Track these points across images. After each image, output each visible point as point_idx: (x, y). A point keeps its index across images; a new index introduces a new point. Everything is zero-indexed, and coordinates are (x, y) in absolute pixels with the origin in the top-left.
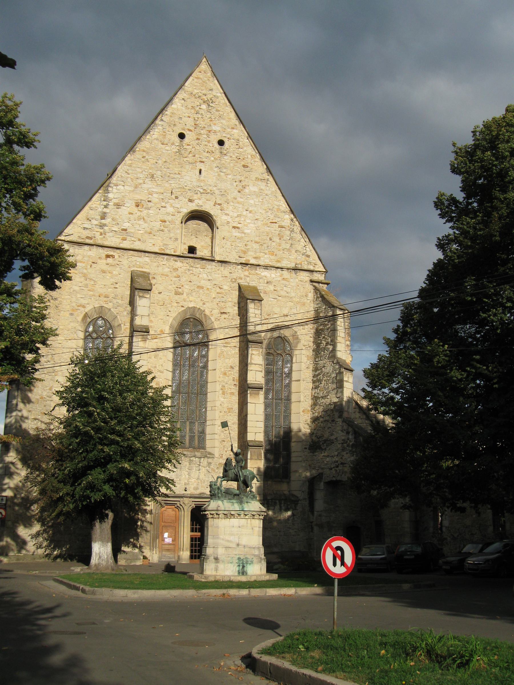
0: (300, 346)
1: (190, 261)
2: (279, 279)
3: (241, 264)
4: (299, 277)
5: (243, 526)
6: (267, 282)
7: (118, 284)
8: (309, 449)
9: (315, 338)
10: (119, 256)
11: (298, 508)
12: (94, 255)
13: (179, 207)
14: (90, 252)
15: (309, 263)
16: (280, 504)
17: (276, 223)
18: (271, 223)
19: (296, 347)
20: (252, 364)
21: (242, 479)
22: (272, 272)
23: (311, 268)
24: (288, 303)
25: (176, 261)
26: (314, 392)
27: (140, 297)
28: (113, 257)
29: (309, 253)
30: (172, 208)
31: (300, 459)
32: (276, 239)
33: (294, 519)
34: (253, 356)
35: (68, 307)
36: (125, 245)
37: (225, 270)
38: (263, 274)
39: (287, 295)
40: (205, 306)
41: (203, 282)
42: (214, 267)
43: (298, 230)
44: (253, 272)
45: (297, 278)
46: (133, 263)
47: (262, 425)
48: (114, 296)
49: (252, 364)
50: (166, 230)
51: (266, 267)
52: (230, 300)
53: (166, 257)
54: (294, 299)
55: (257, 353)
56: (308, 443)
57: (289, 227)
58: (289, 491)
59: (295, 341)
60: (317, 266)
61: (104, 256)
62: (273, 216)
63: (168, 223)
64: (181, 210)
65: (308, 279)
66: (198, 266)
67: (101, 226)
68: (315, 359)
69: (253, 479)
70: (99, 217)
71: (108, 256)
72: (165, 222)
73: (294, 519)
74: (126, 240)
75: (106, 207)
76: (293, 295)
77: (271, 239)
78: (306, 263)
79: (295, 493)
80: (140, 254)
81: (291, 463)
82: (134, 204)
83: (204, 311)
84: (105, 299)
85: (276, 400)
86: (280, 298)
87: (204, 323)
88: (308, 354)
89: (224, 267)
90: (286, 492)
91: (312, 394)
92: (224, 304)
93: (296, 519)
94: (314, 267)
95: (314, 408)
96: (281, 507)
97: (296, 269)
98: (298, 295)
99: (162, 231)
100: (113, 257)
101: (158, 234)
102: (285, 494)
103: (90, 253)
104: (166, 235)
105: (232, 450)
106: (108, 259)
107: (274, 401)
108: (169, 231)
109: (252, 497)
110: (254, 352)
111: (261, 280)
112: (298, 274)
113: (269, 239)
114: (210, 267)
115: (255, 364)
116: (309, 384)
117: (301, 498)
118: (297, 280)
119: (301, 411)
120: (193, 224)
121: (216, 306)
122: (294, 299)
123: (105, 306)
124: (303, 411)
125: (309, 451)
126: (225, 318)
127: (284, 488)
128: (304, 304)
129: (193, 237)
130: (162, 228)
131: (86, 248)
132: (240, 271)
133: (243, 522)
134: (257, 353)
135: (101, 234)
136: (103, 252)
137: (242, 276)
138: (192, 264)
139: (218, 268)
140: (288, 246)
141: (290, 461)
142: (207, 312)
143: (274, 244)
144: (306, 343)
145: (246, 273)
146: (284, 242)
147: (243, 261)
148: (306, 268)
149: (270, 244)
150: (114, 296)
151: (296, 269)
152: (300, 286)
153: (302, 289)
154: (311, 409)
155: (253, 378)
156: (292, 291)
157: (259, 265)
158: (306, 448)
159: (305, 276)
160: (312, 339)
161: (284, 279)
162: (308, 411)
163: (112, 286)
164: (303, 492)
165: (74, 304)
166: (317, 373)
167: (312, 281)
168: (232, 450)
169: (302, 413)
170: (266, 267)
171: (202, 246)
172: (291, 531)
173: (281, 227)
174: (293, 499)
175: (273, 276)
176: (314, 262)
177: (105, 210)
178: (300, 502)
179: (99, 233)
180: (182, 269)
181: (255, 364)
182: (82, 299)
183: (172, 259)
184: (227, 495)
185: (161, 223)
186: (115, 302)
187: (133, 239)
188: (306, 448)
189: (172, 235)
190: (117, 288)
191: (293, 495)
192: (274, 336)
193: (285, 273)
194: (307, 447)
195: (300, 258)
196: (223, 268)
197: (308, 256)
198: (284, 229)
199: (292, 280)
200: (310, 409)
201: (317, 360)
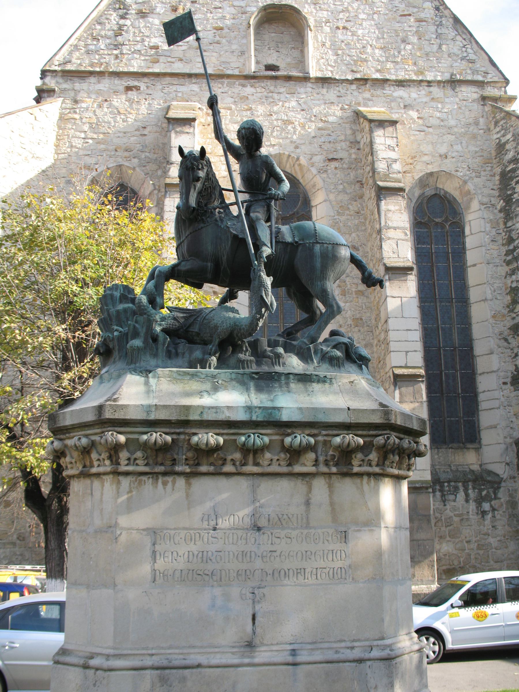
0: (475, 205)
1: (269, 83)
2: (424, 100)
3: (357, 79)
4: (460, 95)
5: (280, 521)
6: (405, 106)
7: (149, 129)
8: (512, 384)
9: (500, 189)
10: (147, 87)
11: (500, 495)
12: (105, 89)
13: (243, 5)
14: (99, 85)
15: (475, 72)
16: (466, 490)
17: (410, 15)
18: (401, 16)
19: (468, 207)
20: (389, 228)
21: (267, 251)
22: (412, 89)
23: (480, 78)
24: (445, 137)
25: (244, 86)
26: (509, 281)
27: (176, 132)
28: (137, 88)
29: (472, 56)
30: (232, 8)
31: (496, 403)
32: (414, 39)
33: (494, 517)
34: (390, 215)
35: (64, 171)
36: (157, 69)
37: (331, 93)
38: (396, 94)
39: (442, 124)
40: (298, 151)
41: (291, 114)
42: (310, 90)
43: (448, 23)
44: (379, 92)
45: (457, 96)
46: (171, 95)
47: (417, 336)
48: (141, 148)
49: (389, 228)
50: (224, 41)
51: (401, 83)
52: (343, 138)
53: (226, 81)
54: (456, 130)
55: (397, 208)
56: (510, 374)
57: (432, 19)
58: (481, 465)
59: (465, 199)
60: (490, 76)
61: (122, 88)
62: (403, 6)
63: (226, 30)
64: (248, 9)
65: (476, 96)
66: (282, 90)
67: (115, 45)
68: (505, 223)
70: (110, 33)
71: (129, 89)
72: (221, 29)
73: (494, 517)
74: (158, 62)
75: (122, 17)
76: (452, 123)
77: (403, 41)
78: (469, 72)
79: (492, 467)
80: (182, 81)
81: (480, 413)
82: (170, 9)
83: (298, 159)
84: (127, 154)
85: (441, 302)
86: (430, 130)
87: (301, 181)
88: (491, 218)
89: (328, 88)
90: (476, 467)
91: (505, 284)
92: (332, 145)
93: (498, 517)
94: (484, 77)
95: (515, 308)
96: (467, 495)
97: (453, 83)
98: (462, 123)
99: (218, 43)
100: (137, 88)
101: (211, 47)
102: (472, 471)
103: (100, 86)
104: (225, 48)
106: (130, 92)
107: (438, 304)
108: (229, 42)
110: (392, 207)
111: (393, 104)
112: (458, 89)
113: (399, 41)
114: (302, 90)
115: (395, 229)
116: (499, 268)
117: (505, 476)
118: (457, 100)
119: (489, 317)
120: (271, 34)
121: (319, 150)
122: (456, 130)
123: (127, 164)
124: (494, 317)
125: (512, 388)
126: (336, 168)
127: (469, 459)
128: (474, 137)
129: (272, 51)
130: (218, 38)
131: (93, 80)
132: (355, 93)
133: (279, 496)
134: (397, 208)
135: (117, 57)
136: (120, 84)
137: (360, 99)
138: (272, 88)
139: (317, 91)
140: (435, 47)
141: (478, 409)
142: (303, 161)
143: (409, 47)
144: (485, 200)
145: (367, 95)
146: (427, 42)
147: (358, 76)
148: (469, 78)
149: (402, 47)
150: (141, 148)
151: (453, 83)
152: (463, 108)
153: (467, 113)
154: (509, 312)
155: (394, 253)
156: (450, 116)
157: (386, 81)
158: (505, 383)
159: (470, 93)
160: (496, 193)
161: (433, 99)
162: (504, 316)
163: (137, 132)
164: (508, 464)
165: (73, 166)
166: (511, 247)
167: (484, 98)
169: (491, 321)
170: (401, 83)
171: (289, 64)
172: (491, 540)
173: (420, 21)
174: (489, 478)
175: (414, 95)
176: (483, 69)
177: (122, 22)
178: (503, 484)
179: (113, 57)
180: (254, 97)
181: (395, 229)
182: (86, 157)
183: (237, 83)
184: (183, 346)
185: (215, 31)
186: (143, 157)
187: (169, 59)
188: (505, 383)
189: (234, 47)
190: (145, 135)
191: (490, 473)
192: (426, 194)
193: (435, 90)
194: (509, 380)
195: (457, 64)
196: (324, 91)
197: (472, 62)
198: (424, 23)
199: (447, 100)
200: (505, 311)
201: (509, 224)
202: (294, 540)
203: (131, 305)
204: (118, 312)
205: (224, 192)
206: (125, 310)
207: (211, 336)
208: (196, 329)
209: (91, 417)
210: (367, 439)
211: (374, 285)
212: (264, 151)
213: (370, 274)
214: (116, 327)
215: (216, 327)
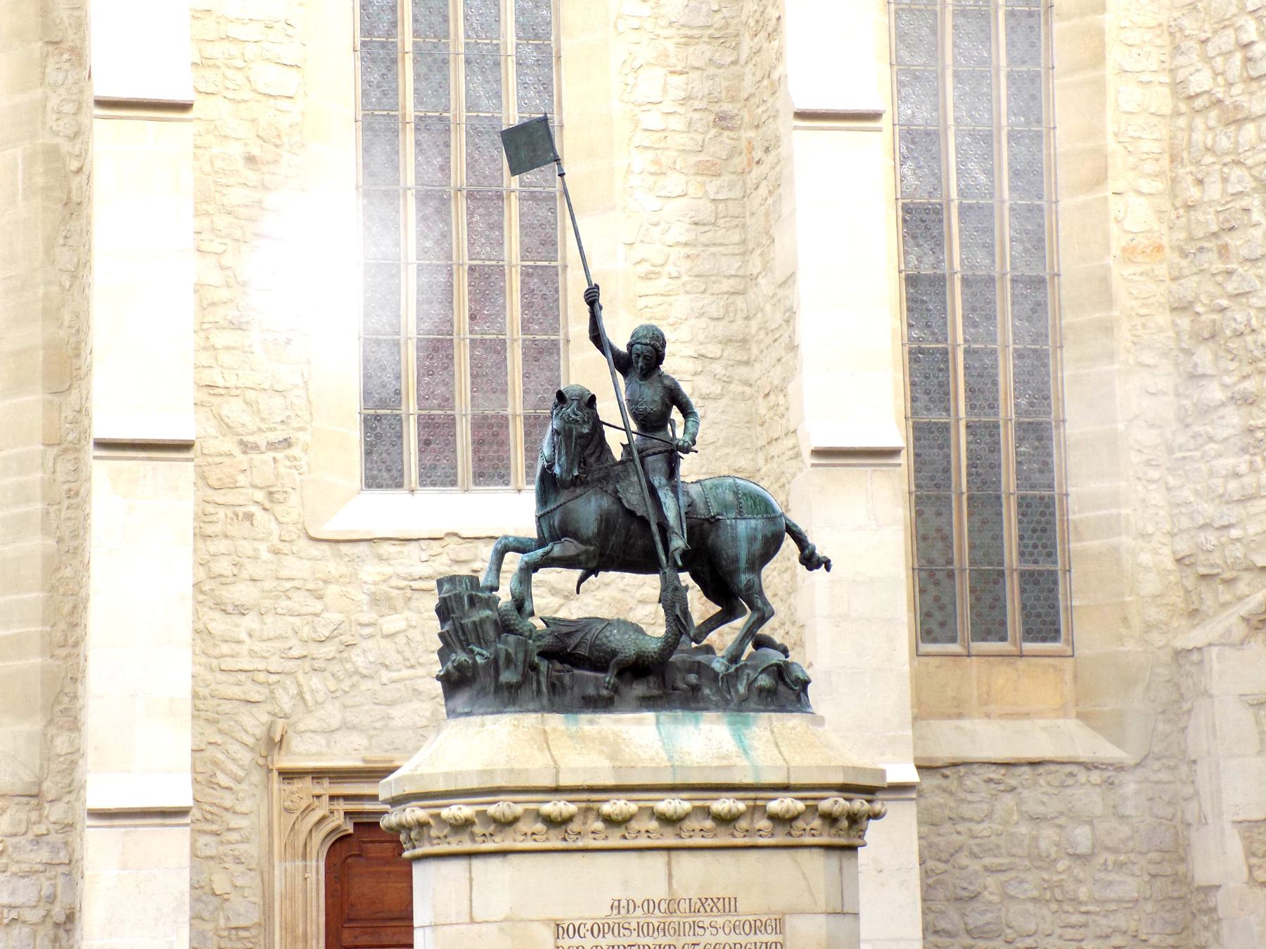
21: (678, 543)
69: (770, 547)
105: (597, 337)
109: (764, 681)
168: (597, 337)
184: (570, 675)
202: (721, 931)
203: (488, 613)
204: (474, 623)
205: (605, 427)
206: (482, 621)
207: (607, 662)
208: (584, 651)
209: (474, 784)
210: (810, 803)
211: (818, 567)
212: (665, 367)
213: (813, 553)
214: (477, 649)
215: (614, 653)
